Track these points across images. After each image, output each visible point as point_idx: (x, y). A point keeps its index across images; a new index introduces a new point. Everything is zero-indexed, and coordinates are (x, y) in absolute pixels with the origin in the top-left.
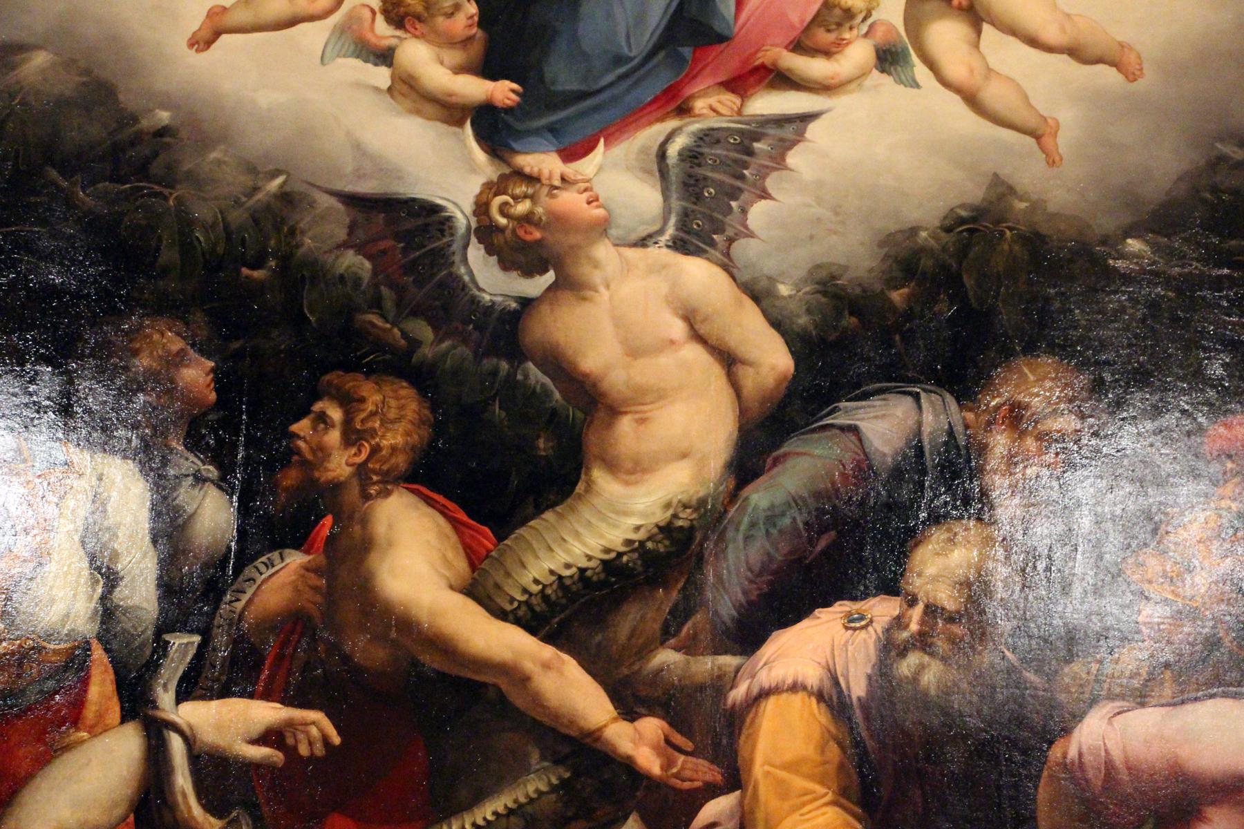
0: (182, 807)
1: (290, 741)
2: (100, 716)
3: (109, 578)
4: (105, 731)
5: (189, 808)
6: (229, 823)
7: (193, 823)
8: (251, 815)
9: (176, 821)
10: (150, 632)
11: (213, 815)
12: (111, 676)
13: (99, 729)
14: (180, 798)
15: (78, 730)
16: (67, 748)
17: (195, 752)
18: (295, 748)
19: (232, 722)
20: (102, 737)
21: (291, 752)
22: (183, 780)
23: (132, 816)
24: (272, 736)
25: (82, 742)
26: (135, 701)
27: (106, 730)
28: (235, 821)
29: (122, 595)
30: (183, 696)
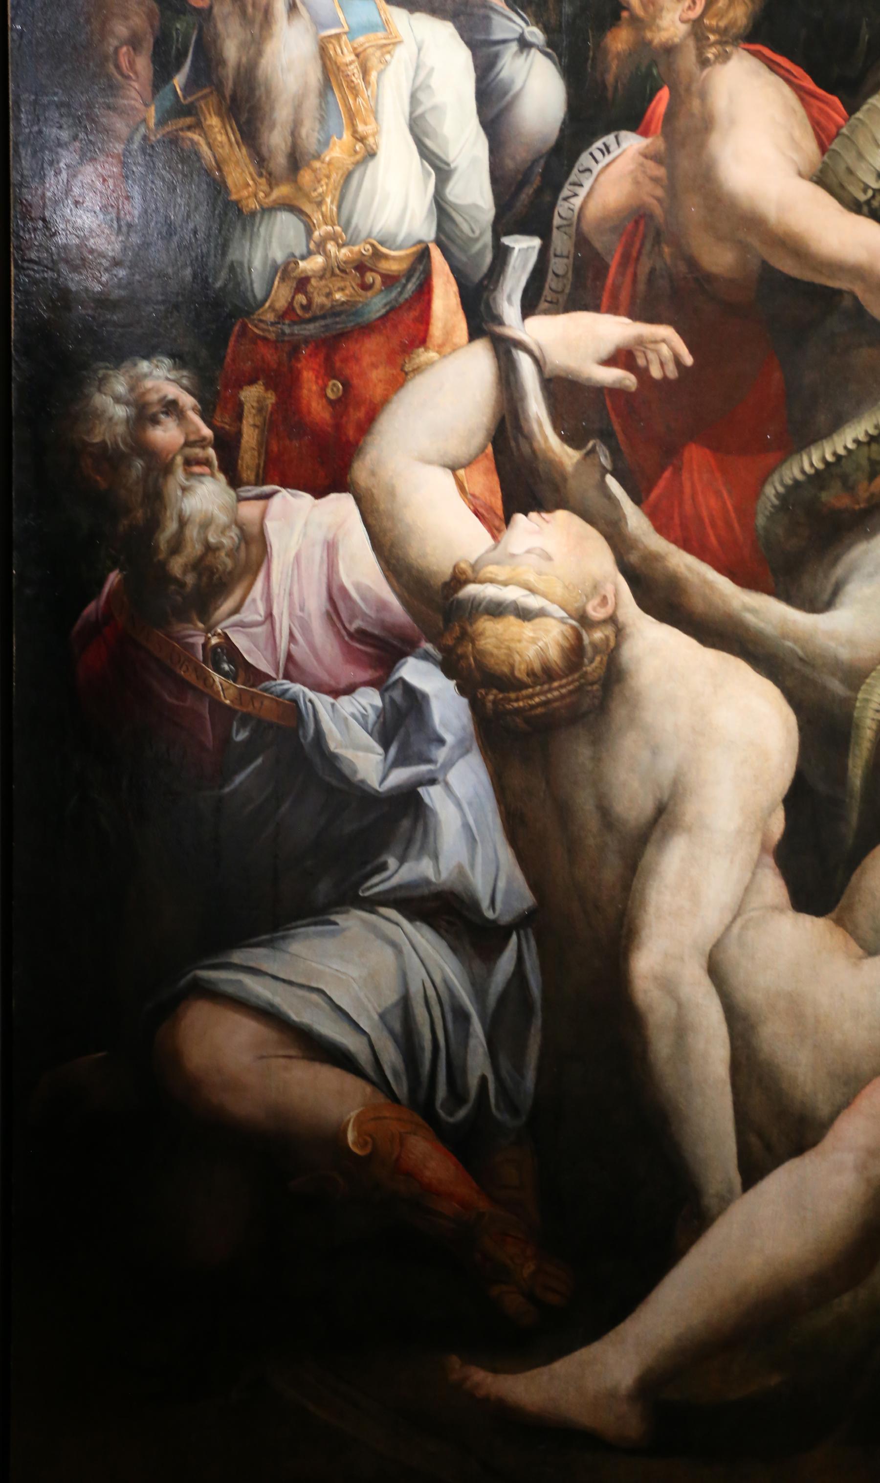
0: (539, 436)
1: (641, 362)
2: (448, 333)
3: (442, 172)
4: (454, 350)
5: (546, 438)
6: (588, 454)
7: (550, 454)
8: (610, 448)
9: (534, 451)
10: (488, 238)
11: (570, 446)
12: (454, 288)
13: (446, 349)
14: (535, 427)
15: (427, 349)
16: (418, 370)
17: (547, 376)
18: (646, 370)
19: (581, 340)
20: (451, 358)
21: (642, 374)
22: (536, 407)
23: (490, 449)
24: (622, 357)
25: (431, 364)
26: (480, 319)
27: (455, 349)
28: (593, 451)
29: (455, 192)
30: (529, 308)
